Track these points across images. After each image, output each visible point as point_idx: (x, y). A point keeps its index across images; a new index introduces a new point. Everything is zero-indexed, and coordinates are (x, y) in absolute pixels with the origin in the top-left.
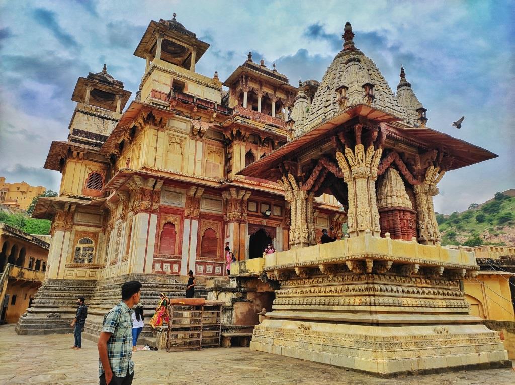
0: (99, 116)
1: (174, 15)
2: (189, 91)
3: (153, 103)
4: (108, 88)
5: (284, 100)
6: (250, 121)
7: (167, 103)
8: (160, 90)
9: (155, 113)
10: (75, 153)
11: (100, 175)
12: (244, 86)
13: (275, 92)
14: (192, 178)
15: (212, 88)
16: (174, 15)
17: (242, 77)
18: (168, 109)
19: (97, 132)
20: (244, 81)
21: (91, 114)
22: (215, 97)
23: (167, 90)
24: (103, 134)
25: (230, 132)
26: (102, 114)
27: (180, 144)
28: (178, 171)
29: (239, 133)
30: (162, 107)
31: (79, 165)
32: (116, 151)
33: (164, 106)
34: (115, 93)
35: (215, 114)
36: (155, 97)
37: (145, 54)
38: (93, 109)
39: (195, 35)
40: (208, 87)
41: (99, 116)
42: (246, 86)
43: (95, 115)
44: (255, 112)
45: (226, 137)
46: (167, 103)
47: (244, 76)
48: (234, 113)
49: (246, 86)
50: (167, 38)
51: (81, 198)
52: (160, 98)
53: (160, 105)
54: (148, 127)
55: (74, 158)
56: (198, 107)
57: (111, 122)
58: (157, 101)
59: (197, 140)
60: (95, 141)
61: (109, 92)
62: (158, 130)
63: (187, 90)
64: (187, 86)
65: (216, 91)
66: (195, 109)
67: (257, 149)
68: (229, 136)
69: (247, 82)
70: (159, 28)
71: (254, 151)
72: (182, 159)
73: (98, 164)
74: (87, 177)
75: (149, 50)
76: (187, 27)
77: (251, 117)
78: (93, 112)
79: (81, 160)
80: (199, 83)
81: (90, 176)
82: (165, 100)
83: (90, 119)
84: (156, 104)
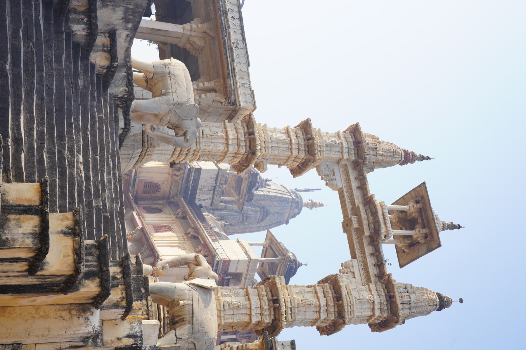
0: (215, 187)
4: (245, 190)
10: (178, 173)
11: (158, 191)
12: (241, 336)
19: (199, 187)
20: (246, 335)
21: (216, 180)
24: (198, 191)
26: (217, 189)
31: (166, 175)
32: (180, 214)
34: (240, 195)
37: (268, 241)
38: (222, 182)
41: (215, 187)
43: (216, 183)
47: (250, 335)
49: (242, 337)
50: (279, 265)
51: (135, 180)
52: (223, 266)
53: (217, 267)
55: (173, 172)
57: (211, 196)
60: (191, 186)
61: (242, 191)
64: (237, 285)
73: (168, 189)
74: (155, 182)
75: (272, 246)
78: (218, 182)
79: (172, 177)
81: (156, 184)
82: (222, 270)
83: (212, 180)
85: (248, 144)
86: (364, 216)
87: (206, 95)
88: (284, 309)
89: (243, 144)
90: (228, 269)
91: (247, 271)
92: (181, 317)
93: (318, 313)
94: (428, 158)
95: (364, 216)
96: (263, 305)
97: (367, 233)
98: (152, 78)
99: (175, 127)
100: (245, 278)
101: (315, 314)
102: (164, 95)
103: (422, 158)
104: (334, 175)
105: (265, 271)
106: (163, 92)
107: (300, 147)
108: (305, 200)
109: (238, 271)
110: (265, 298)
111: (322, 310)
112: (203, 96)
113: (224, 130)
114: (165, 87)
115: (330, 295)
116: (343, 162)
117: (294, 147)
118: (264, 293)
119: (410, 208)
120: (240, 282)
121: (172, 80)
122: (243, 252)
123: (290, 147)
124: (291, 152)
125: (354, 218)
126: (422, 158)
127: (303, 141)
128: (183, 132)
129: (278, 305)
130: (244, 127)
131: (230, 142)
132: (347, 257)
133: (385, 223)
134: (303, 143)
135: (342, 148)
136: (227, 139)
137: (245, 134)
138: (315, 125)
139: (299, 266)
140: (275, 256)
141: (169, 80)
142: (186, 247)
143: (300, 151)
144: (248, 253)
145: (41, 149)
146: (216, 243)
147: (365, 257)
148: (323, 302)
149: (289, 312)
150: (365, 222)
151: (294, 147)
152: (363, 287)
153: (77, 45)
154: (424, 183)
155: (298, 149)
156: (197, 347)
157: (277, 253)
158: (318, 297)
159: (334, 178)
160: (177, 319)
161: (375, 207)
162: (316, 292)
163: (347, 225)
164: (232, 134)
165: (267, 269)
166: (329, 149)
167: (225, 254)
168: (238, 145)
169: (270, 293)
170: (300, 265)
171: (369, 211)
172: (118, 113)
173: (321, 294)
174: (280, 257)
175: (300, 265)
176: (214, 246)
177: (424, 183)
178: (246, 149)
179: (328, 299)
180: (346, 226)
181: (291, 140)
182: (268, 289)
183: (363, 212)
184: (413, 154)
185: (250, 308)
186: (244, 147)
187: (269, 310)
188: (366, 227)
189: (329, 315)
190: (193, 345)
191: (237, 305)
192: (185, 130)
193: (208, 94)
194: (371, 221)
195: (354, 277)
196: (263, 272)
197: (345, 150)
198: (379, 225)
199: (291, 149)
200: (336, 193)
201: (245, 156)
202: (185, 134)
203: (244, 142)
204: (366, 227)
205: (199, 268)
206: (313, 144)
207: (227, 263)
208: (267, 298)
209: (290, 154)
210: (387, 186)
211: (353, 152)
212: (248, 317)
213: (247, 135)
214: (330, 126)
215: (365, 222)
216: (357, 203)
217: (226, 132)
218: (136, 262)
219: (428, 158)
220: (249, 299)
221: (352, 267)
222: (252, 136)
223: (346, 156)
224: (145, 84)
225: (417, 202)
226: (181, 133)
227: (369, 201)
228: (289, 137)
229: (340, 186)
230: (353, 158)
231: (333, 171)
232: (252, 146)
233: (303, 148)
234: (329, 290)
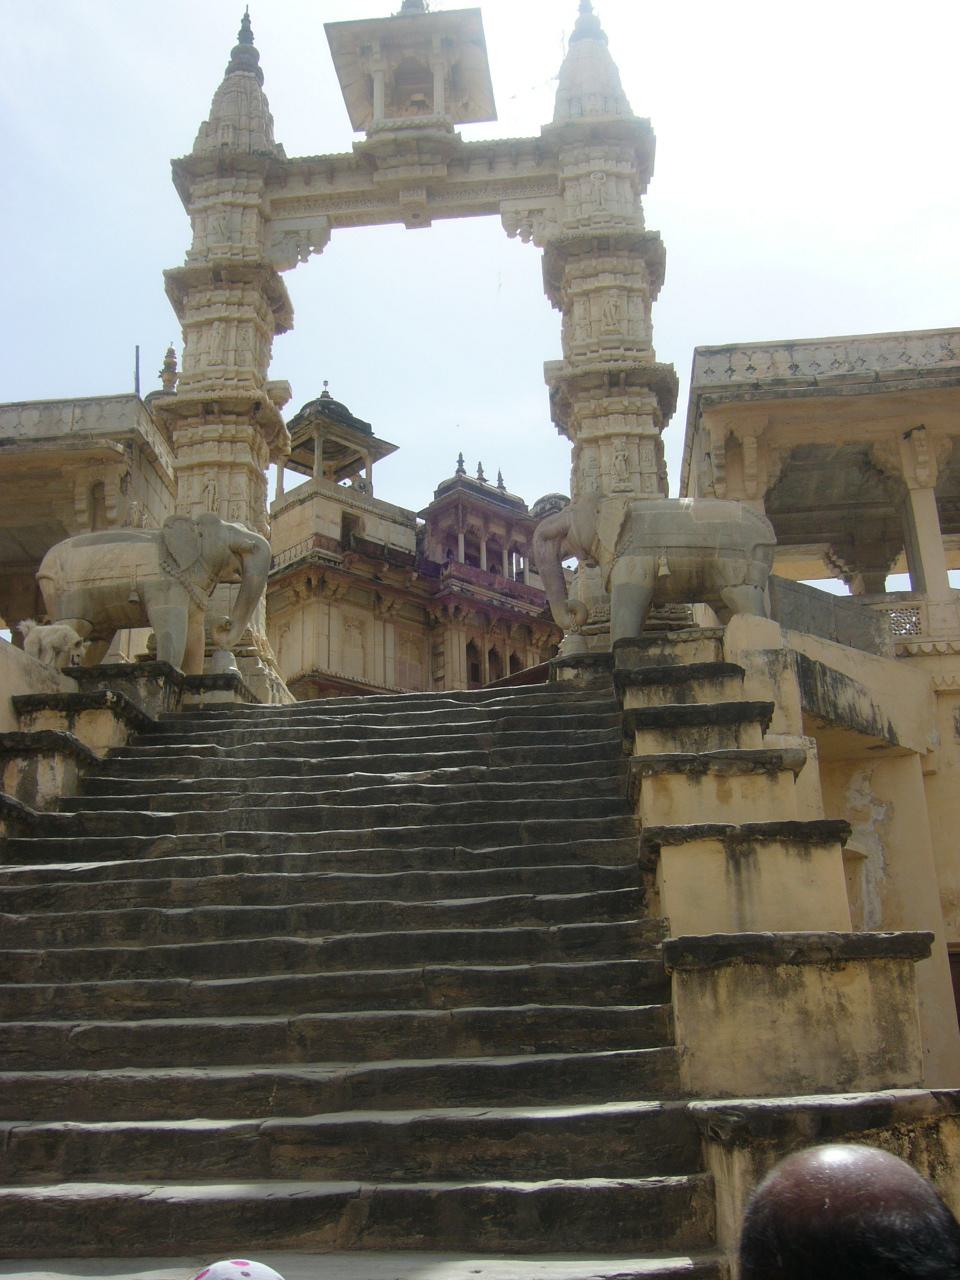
1: (326, 383)
2: (367, 532)
3: (319, 558)
5: (522, 545)
6: (471, 588)
7: (340, 557)
8: (326, 533)
9: (328, 575)
12: (461, 525)
13: (509, 532)
14: (383, 688)
15: (401, 524)
16: (326, 383)
17: (456, 507)
18: (341, 566)
22: (404, 540)
23: (336, 533)
25: (441, 608)
27: (361, 626)
28: (359, 678)
29: (457, 609)
30: (332, 564)
33: (335, 562)
35: (415, 575)
36: (321, 546)
39: (369, 426)
40: (395, 522)
42: (463, 522)
44: (478, 570)
45: (432, 617)
46: (340, 557)
47: (460, 506)
48: (446, 573)
49: (463, 522)
52: (328, 549)
53: (329, 561)
54: (313, 599)
56: (390, 564)
58: (327, 555)
59: (385, 621)
62: (329, 605)
63: (364, 530)
64: (363, 524)
65: (409, 531)
66: (386, 568)
67: (483, 638)
68: (439, 614)
69: (464, 516)
70: (318, 421)
71: (478, 642)
72: (365, 655)
76: (357, 412)
77: (474, 580)
80: (382, 517)
82: (335, 552)
84: (324, 559)
85: (233, 418)
86: (404, 174)
87: (112, 508)
88: (629, 364)
89: (232, 429)
90: (335, 540)
91: (340, 501)
92: (694, 574)
93: (632, 294)
94: (246, 20)
95: (404, 174)
96: (620, 408)
97: (442, 171)
98: (91, 623)
99: (217, 575)
100: (351, 506)
101: (635, 299)
102: (141, 597)
103: (246, 34)
104: (297, 233)
105: (333, 469)
106: (136, 598)
107: (236, 300)
108: (159, 385)
109: (339, 520)
110: (605, 402)
111: (628, 284)
112: (112, 515)
113: (196, 471)
114: (119, 593)
115: (594, 262)
116: (268, 210)
117: (234, 313)
118: (593, 404)
119: (379, 70)
120: (358, 518)
121: (103, 575)
122: (298, 508)
123: (236, 323)
124: (248, 321)
125: (404, 198)
126: (246, 34)
127: (221, 292)
128: (233, 557)
129: (623, 375)
130: (189, 425)
131: (229, 458)
132: (491, 225)
133: (419, 127)
134: (227, 293)
135: (233, 205)
136: (220, 465)
137: (206, 423)
138: (178, 261)
139: (328, 397)
140: (308, 445)
141: (103, 584)
142: (283, 621)
143: (247, 300)
144: (301, 497)
145: (468, 861)
146: (276, 560)
147: (496, 182)
148: (606, 280)
149: (634, 353)
150: (417, 173)
151: (234, 313)
152: (568, 194)
153: (86, 786)
154: (328, 27)
155: (241, 304)
156: (761, 542)
157: (304, 438)
158: (598, 290)
159: (303, 234)
160: (695, 582)
161: (384, 144)
162: (586, 294)
163: (415, 216)
164: (210, 453)
165: (331, 463)
166: (237, 236)
167: (293, 550)
168: (233, 441)
169: (592, 392)
170: (325, 394)
171: (393, 162)
172: (198, 705)
173: (591, 284)
174: (315, 435)
175: (325, 394)
176: (283, 566)
177: (328, 27)
178: (243, 424)
179: (600, 268)
180: (417, 218)
181: (220, 320)
182: (581, 395)
183: (391, 176)
184: (235, 53)
185: (628, 435)
186: (240, 428)
187: (629, 394)
188: (429, 172)
189: (636, 269)
190: (758, 549)
191: (623, 462)
192: (229, 552)
193: (109, 502)
194: (416, 158)
195: (541, 211)
196: (336, 472)
197: (241, 199)
198: (427, 139)
199: (240, 321)
200: (335, 233)
201: (258, 428)
202: (238, 552)
203: (228, 427)
204: (429, 172)
205: (573, 531)
206: (232, 268)
207: (323, 540)
208: (605, 399)
209: (251, 324)
210: (313, 120)
211: (244, 181)
212: (645, 442)
213: (210, 418)
214: (171, 235)
215: (417, 173)
216: (366, 187)
217: (201, 465)
218: (573, 667)
219: (246, 20)
220: (608, 437)
221: (517, 213)
222: (216, 408)
223: (254, 199)
224: (101, 643)
225: (366, 51)
226: (235, 562)
227: (365, 160)
228: (210, 323)
229: (323, 221)
230: (260, 183)
231: (287, 233)
232: (237, 410)
233: (238, 293)
234: (583, 265)
